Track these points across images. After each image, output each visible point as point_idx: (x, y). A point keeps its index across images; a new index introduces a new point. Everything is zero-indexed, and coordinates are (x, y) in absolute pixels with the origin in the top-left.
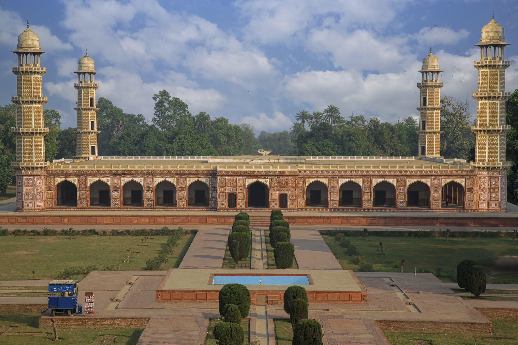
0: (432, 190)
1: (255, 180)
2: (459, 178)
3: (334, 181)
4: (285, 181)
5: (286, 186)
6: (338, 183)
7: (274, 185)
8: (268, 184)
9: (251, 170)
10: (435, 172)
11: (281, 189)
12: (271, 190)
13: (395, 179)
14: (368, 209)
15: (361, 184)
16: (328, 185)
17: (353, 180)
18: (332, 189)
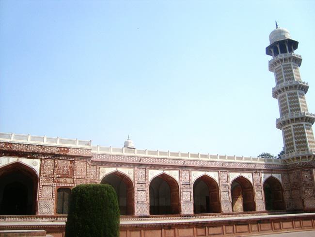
0: (255, 187)
1: (12, 160)
2: (276, 173)
3: (141, 172)
4: (69, 165)
5: (71, 174)
6: (146, 176)
7: (50, 172)
8: (37, 168)
9: (8, 140)
10: (255, 164)
11: (61, 180)
12: (42, 181)
13: (217, 173)
14: (188, 216)
15: (177, 179)
16: (132, 179)
17: (167, 172)
18: (139, 186)
